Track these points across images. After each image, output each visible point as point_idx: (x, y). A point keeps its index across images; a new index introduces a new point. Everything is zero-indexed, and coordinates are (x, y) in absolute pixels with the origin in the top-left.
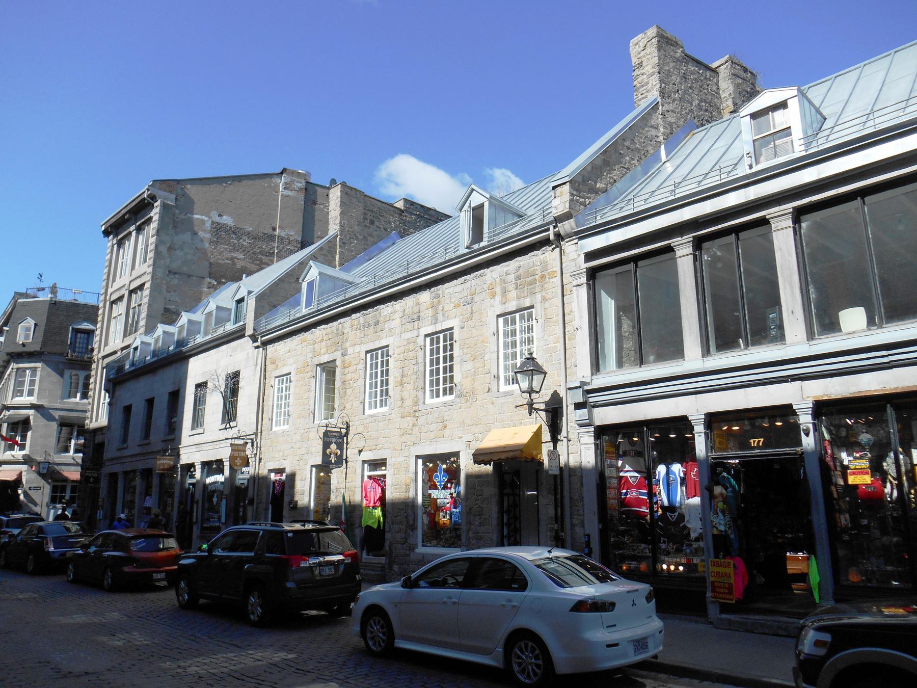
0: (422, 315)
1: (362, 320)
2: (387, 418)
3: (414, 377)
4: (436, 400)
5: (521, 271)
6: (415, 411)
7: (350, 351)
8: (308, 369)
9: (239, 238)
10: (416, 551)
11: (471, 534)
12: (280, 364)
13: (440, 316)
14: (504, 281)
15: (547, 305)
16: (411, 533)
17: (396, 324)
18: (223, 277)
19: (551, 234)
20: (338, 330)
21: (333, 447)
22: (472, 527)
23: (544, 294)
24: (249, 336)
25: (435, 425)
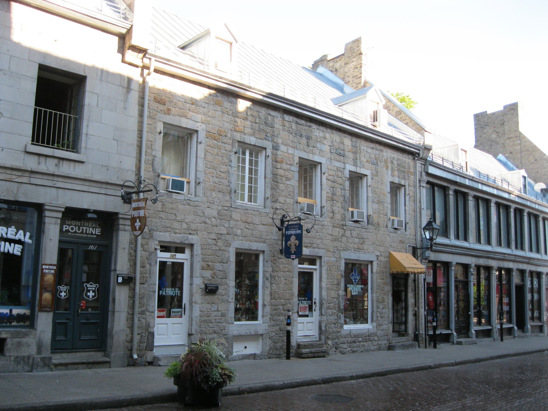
1: (294, 126)
3: (342, 199)
6: (343, 225)
7: (283, 148)
13: (358, 162)
20: (266, 119)
21: (293, 238)
22: (379, 310)
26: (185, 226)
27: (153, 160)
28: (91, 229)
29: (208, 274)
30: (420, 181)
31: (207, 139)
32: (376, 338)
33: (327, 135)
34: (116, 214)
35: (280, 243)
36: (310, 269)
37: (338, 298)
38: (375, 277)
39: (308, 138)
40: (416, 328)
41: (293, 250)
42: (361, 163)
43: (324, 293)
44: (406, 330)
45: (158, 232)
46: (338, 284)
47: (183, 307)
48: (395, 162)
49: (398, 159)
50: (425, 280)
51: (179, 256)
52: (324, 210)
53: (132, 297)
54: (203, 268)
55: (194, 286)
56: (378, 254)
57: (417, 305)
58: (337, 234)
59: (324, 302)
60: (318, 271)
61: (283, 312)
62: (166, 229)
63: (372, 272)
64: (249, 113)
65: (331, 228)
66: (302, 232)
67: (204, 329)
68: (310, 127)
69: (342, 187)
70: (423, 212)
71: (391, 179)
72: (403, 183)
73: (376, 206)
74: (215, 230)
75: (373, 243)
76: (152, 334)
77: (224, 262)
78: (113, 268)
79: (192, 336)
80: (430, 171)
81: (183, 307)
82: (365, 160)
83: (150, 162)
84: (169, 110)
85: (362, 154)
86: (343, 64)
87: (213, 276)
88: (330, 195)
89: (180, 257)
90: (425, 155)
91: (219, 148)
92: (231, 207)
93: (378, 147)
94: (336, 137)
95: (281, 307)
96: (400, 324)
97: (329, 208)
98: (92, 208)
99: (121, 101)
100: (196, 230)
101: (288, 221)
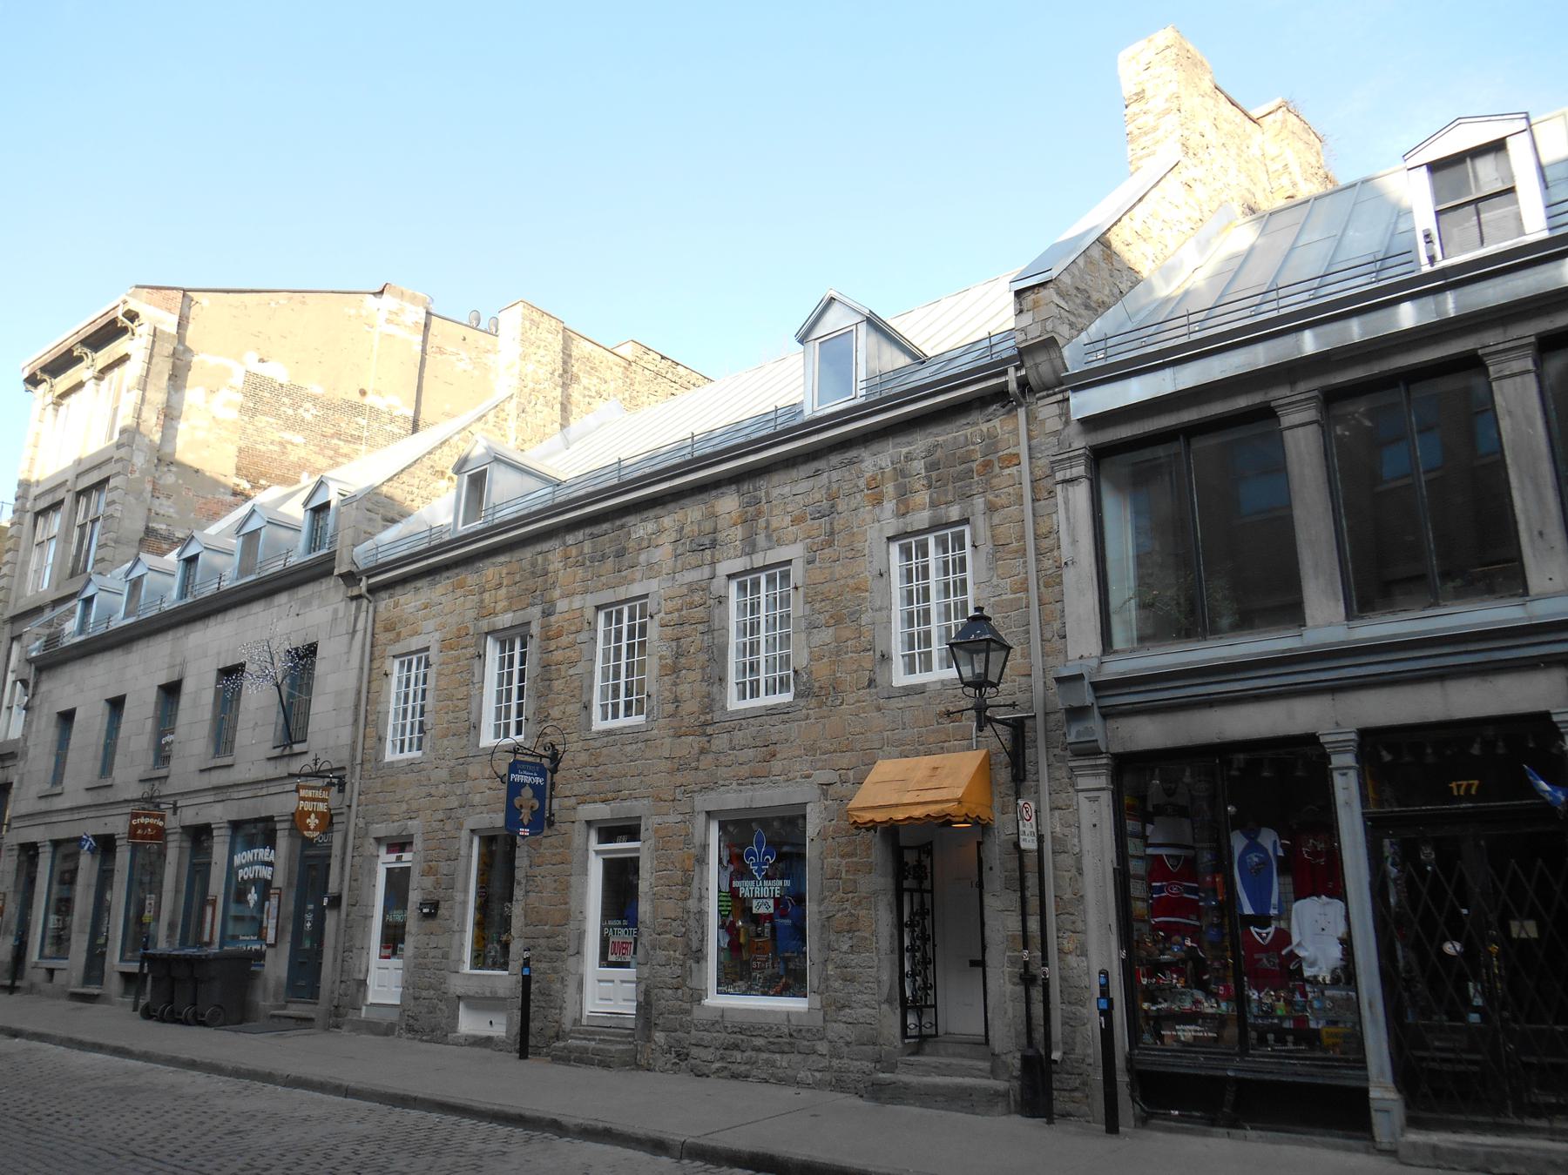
0: (721, 536)
1: (587, 547)
2: (642, 737)
3: (703, 657)
4: (750, 703)
5: (939, 453)
6: (705, 724)
7: (562, 605)
8: (469, 640)
9: (296, 406)
10: (707, 1002)
11: (831, 970)
12: (404, 632)
13: (761, 540)
14: (900, 473)
15: (996, 519)
16: (694, 966)
17: (663, 553)
18: (263, 475)
19: (1012, 377)
20: (534, 564)
21: (527, 793)
23: (991, 497)
24: (341, 575)
25: (751, 752)
29: (428, 882)
32: (822, 1047)
37: (684, 923)
41: (525, 816)
49: (929, 453)
56: (826, 776)
58: (685, 752)
61: (547, 952)
62: (386, 817)
65: (668, 740)
68: (622, 526)
69: (700, 627)
72: (954, 513)
73: (825, 636)
74: (444, 804)
75: (811, 749)
76: (363, 984)
84: (399, 634)
91: (457, 659)
93: (835, 459)
95: (542, 941)
97: (667, 694)
100: (418, 811)
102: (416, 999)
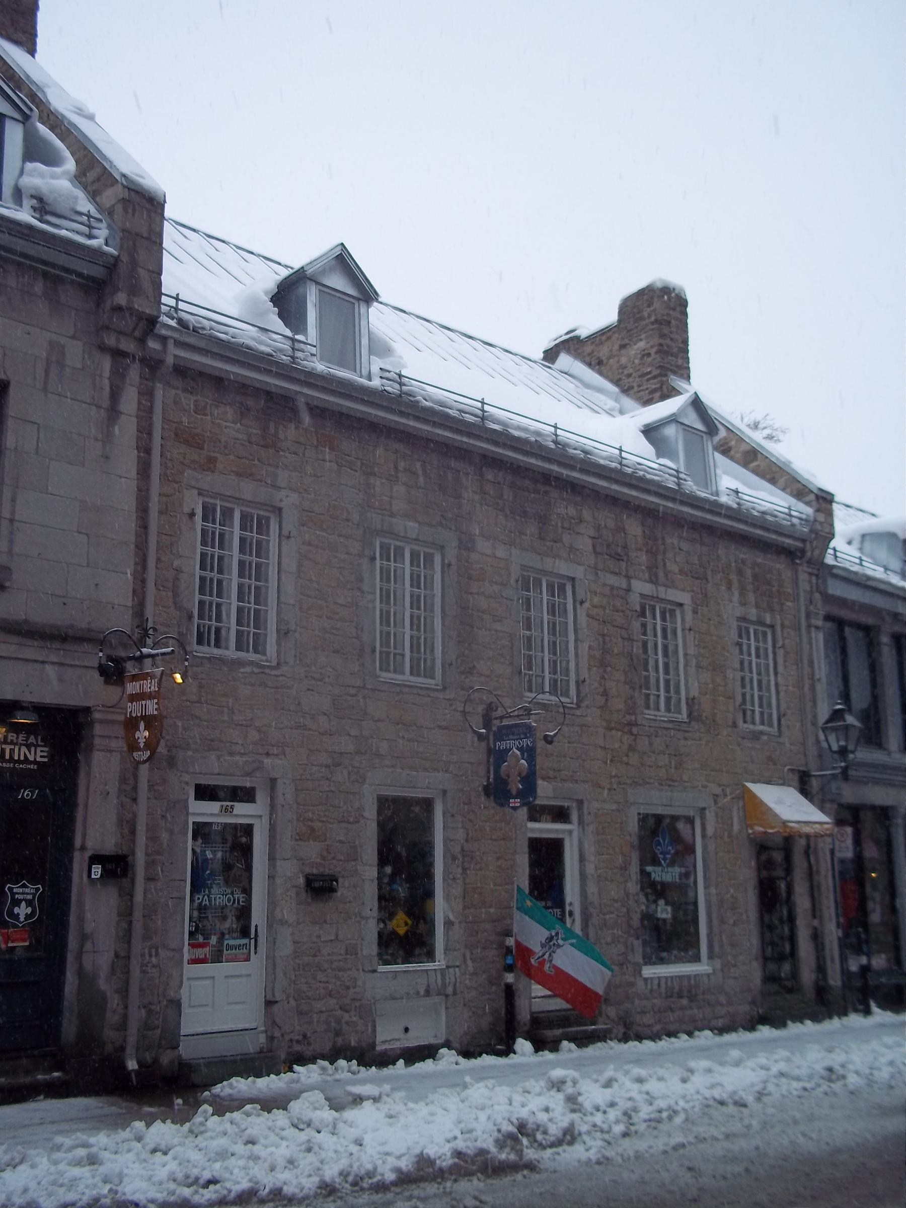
1: (508, 494)
6: (630, 724)
7: (483, 545)
13: (661, 574)
26: (254, 735)
27: (176, 579)
28: (24, 749)
30: (808, 615)
31: (302, 528)
32: (722, 999)
33: (586, 514)
34: (87, 710)
35: (482, 770)
36: (557, 831)
38: (712, 848)
39: (543, 520)
40: (821, 969)
41: (516, 785)
42: (666, 575)
43: (592, 889)
44: (795, 974)
45: (190, 753)
46: (624, 868)
47: (253, 936)
48: (748, 572)
50: (832, 852)
51: (241, 808)
52: (585, 689)
53: (126, 914)
54: (300, 838)
55: (278, 881)
56: (718, 790)
57: (818, 913)
59: (591, 910)
60: (575, 835)
63: (704, 836)
64: (402, 465)
66: (534, 742)
67: (304, 988)
69: (624, 633)
70: (819, 687)
71: (739, 611)
77: (351, 820)
78: (78, 842)
79: (275, 1008)
80: (830, 591)
81: (253, 936)
82: (677, 570)
83: (170, 585)
84: (212, 460)
85: (670, 555)
86: (616, 347)
87: (325, 854)
88: (597, 654)
89: (242, 812)
90: (817, 552)
92: (364, 687)
94: (606, 517)
96: (781, 958)
97: (596, 685)
98: (27, 698)
99: (96, 439)
101: (501, 718)
102: (300, 1013)
